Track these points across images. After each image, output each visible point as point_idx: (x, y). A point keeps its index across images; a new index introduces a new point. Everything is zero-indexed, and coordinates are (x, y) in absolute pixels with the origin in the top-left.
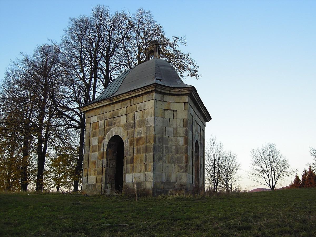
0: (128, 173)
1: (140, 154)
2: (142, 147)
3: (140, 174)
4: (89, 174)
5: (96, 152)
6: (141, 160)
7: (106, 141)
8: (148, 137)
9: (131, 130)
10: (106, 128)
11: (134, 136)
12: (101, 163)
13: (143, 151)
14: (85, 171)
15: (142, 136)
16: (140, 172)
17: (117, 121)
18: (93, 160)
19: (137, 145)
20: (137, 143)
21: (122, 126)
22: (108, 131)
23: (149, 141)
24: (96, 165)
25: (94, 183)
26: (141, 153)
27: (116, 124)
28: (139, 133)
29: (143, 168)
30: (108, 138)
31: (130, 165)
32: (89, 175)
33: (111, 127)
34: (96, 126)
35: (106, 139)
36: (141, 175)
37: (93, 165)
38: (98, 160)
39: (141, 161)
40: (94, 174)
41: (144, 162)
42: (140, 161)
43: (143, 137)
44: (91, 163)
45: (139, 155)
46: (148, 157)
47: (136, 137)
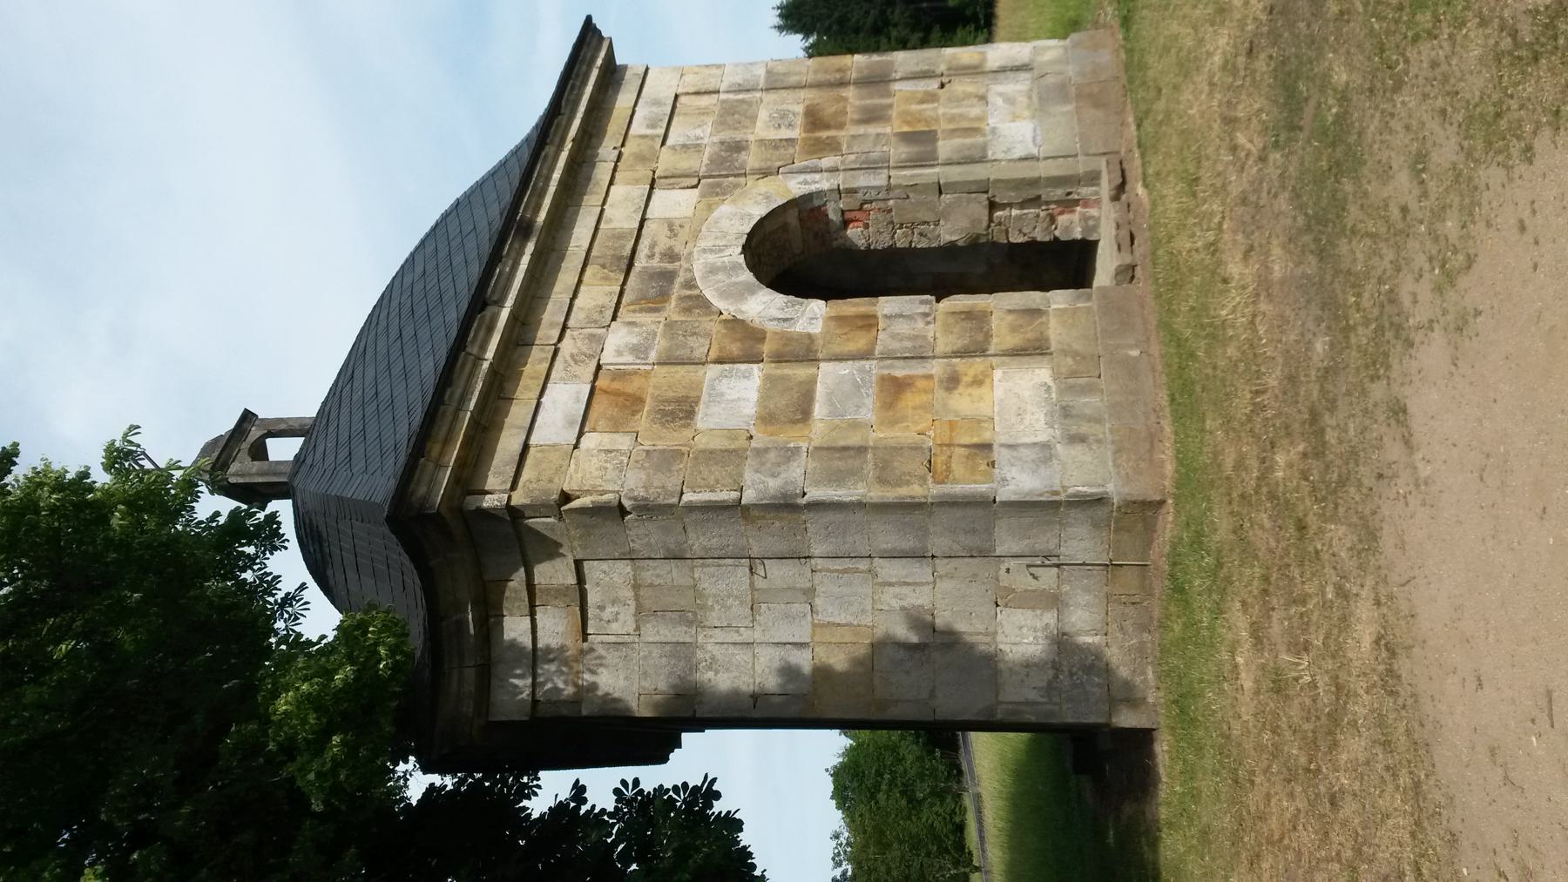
0: (984, 148)
1: (890, 106)
2: (858, 103)
3: (992, 98)
4: (975, 440)
5: (812, 382)
6: (922, 102)
7: (764, 306)
8: (821, 77)
9: (751, 159)
10: (672, 309)
11: (790, 141)
12: (902, 327)
13: (882, 96)
14: (949, 470)
15: (800, 109)
16: (983, 98)
17: (664, 243)
18: (869, 402)
19: (841, 126)
20: (827, 127)
21: (710, 208)
22: (698, 297)
23: (839, 70)
24: (916, 369)
25: (1051, 383)
27: (679, 248)
28: (782, 119)
29: (961, 86)
30: (743, 293)
31: (940, 143)
32: (986, 436)
33: (679, 280)
34: (617, 394)
35: (744, 308)
36: (1000, 94)
37: (910, 400)
38: (878, 349)
39: (930, 98)
40: (978, 382)
41: (933, 85)
42: (924, 106)
43: (807, 103)
44: (893, 423)
45: (894, 113)
46: (917, 69)
47: (796, 133)
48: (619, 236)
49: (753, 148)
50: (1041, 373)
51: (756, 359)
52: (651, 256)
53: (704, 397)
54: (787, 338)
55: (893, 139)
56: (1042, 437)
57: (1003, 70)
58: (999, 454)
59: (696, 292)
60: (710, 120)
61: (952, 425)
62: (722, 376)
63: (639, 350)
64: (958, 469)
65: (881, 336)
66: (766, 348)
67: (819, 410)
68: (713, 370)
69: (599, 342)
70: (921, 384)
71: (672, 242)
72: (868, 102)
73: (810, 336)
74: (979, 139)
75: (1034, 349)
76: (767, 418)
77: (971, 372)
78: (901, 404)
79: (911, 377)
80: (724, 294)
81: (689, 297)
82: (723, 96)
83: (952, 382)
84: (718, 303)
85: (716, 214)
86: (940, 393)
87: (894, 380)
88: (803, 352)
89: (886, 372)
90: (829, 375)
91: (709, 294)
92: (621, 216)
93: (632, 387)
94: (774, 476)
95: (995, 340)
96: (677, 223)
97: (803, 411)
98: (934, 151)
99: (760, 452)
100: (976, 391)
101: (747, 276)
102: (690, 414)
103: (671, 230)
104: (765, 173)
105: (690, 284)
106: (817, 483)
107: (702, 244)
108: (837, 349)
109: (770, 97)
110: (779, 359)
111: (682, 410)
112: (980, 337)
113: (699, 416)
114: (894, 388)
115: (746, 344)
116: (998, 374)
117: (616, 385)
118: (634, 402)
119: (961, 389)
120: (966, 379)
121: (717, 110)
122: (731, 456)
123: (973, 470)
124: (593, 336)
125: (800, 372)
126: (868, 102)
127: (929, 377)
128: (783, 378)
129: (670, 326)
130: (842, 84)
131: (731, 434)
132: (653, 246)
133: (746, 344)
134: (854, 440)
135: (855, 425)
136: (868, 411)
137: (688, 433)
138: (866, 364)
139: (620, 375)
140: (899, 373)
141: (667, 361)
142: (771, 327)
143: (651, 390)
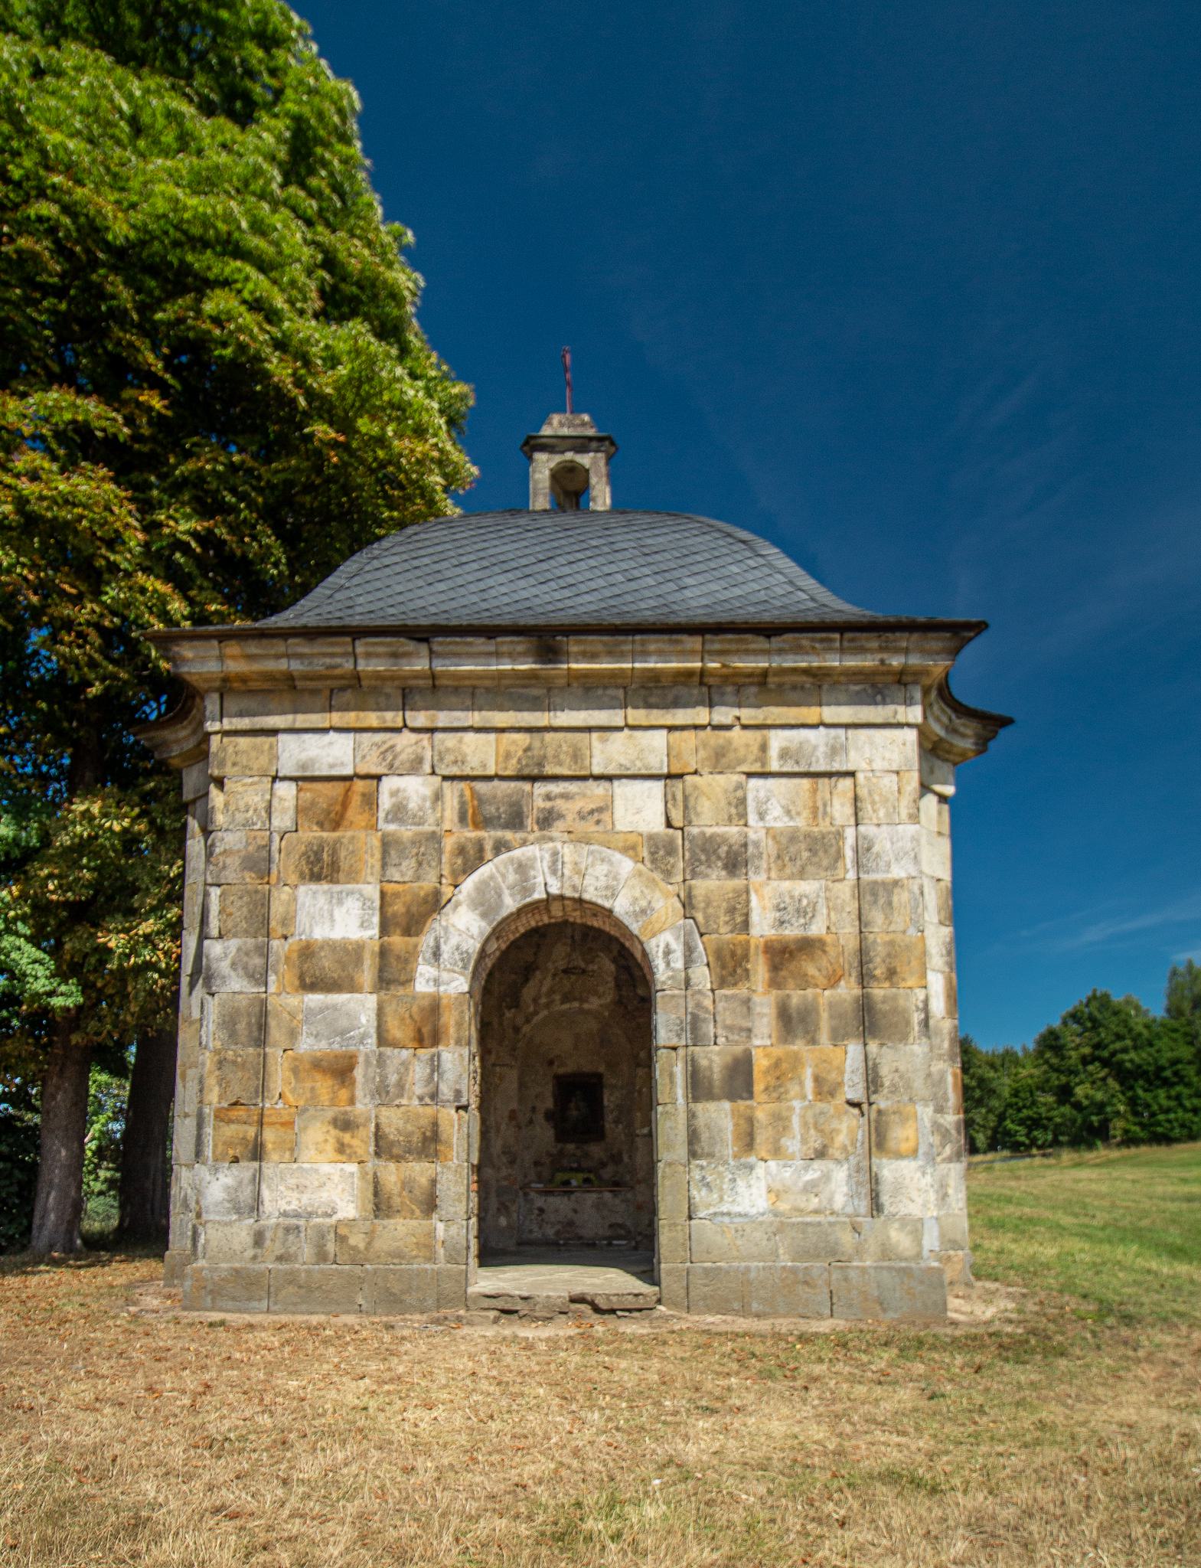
1: (813, 1041)
5: (353, 988)
9: (713, 884)
15: (817, 929)
16: (821, 1154)
19: (775, 983)
20: (775, 968)
21: (629, 849)
26: (824, 1036)
30: (484, 903)
31: (726, 1105)
32: (273, 1156)
34: (345, 805)
35: (463, 909)
37: (324, 1086)
38: (388, 1051)
40: (341, 1148)
44: (295, 1071)
45: (798, 1046)
48: (576, 756)
49: (738, 883)
50: (348, 1210)
51: (385, 929)
52: (548, 797)
53: (337, 888)
54: (408, 960)
55: (738, 1049)
56: (268, 1206)
57: (874, 1181)
58: (247, 1168)
59: (488, 855)
60: (801, 823)
61: (289, 1124)
62: (365, 900)
63: (399, 813)
64: (230, 1131)
65: (405, 1054)
66: (397, 940)
67: (315, 999)
68: (372, 891)
69: (414, 767)
70: (344, 1094)
71: (570, 817)
72: (825, 1015)
73: (410, 980)
74: (729, 1150)
75: (380, 1204)
76: (307, 951)
77: (355, 1142)
78: (318, 1076)
79: (353, 1083)
80: (482, 888)
81: (481, 850)
82: (850, 834)
83: (345, 1124)
84: (469, 884)
85: (617, 856)
86: (330, 1114)
87: (351, 1068)
88: (391, 973)
89: (361, 1059)
90: (361, 1007)
91: (484, 871)
92: (605, 753)
93: (353, 813)
94: (233, 965)
95: (392, 1166)
96: (606, 816)
97: (310, 984)
98: (711, 1096)
99: (264, 952)
100: (330, 1147)
101: (511, 904)
102: (316, 877)
103: (592, 812)
104: (688, 904)
105: (500, 847)
106: (222, 1005)
107: (567, 852)
108: (389, 1009)
109: (844, 891)
110: (384, 953)
111: (322, 868)
112: (395, 1151)
113: (314, 887)
114: (341, 1070)
115: (408, 918)
116: (352, 1167)
117: (356, 800)
118: (335, 820)
119: (334, 1132)
120: (347, 1137)
121: (824, 826)
122: (261, 921)
123: (229, 1144)
124: (420, 760)
125: (367, 975)
126: (825, 1015)
127: (352, 1101)
128: (358, 960)
129: (434, 838)
130: (864, 978)
131: (288, 920)
132: (566, 796)
133: (408, 918)
134: (276, 1033)
135: (293, 1034)
136: (306, 1045)
137: (293, 879)
138: (372, 1041)
139: (371, 801)
140: (359, 1073)
141: (387, 844)
142: (426, 941)
143: (349, 834)
